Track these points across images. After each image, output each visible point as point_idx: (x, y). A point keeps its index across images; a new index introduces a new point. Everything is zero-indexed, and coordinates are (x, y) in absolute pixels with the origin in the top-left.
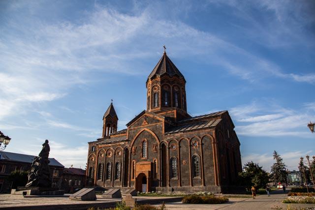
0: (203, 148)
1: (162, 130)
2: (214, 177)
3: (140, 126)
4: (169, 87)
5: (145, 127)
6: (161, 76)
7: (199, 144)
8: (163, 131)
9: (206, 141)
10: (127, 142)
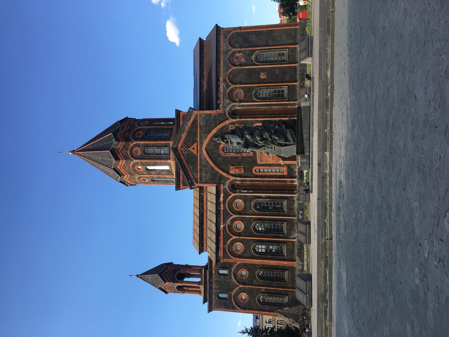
1: (210, 115)
3: (197, 158)
4: (140, 130)
5: (201, 147)
7: (240, 52)
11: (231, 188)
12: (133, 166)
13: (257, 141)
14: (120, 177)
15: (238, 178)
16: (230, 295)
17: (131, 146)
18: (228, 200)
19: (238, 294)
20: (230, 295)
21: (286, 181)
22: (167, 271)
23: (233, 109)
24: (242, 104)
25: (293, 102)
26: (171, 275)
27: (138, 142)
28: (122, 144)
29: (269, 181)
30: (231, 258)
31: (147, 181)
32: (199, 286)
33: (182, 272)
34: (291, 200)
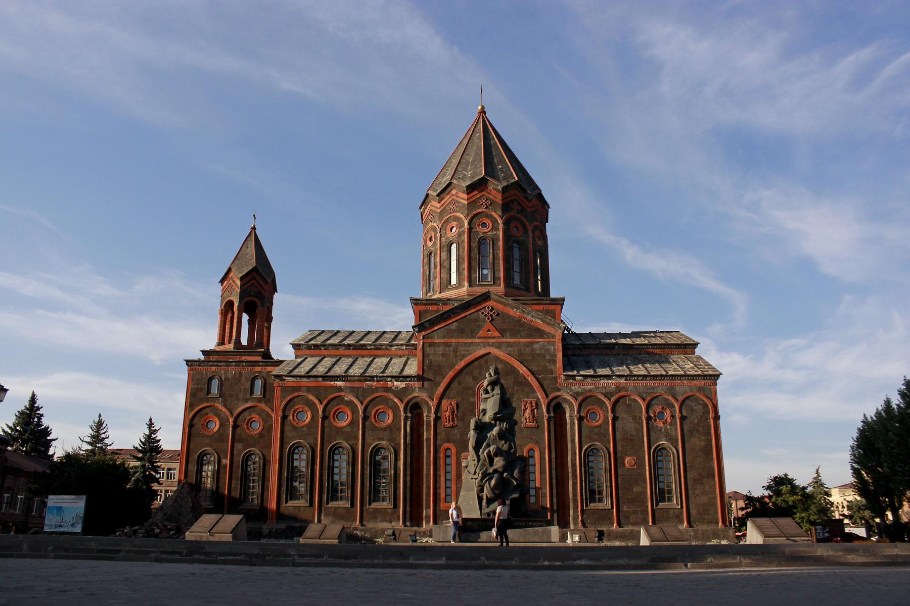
0: (685, 427)
1: (554, 362)
2: (715, 505)
3: (474, 337)
5: (493, 345)
6: (503, 188)
7: (673, 416)
8: (559, 364)
9: (692, 410)
10: (417, 384)
11: (414, 401)
12: (456, 219)
13: (488, 445)
14: (435, 194)
15: (433, 416)
16: (214, 399)
17: (493, 214)
18: (392, 397)
19: (218, 414)
20: (214, 399)
21: (428, 507)
22: (261, 281)
23: (566, 406)
24: (576, 422)
25: (580, 519)
26: (254, 291)
27: (501, 227)
28: (499, 199)
29: (428, 475)
30: (281, 402)
31: (430, 244)
32: (233, 341)
33: (259, 310)
34: (390, 516)
